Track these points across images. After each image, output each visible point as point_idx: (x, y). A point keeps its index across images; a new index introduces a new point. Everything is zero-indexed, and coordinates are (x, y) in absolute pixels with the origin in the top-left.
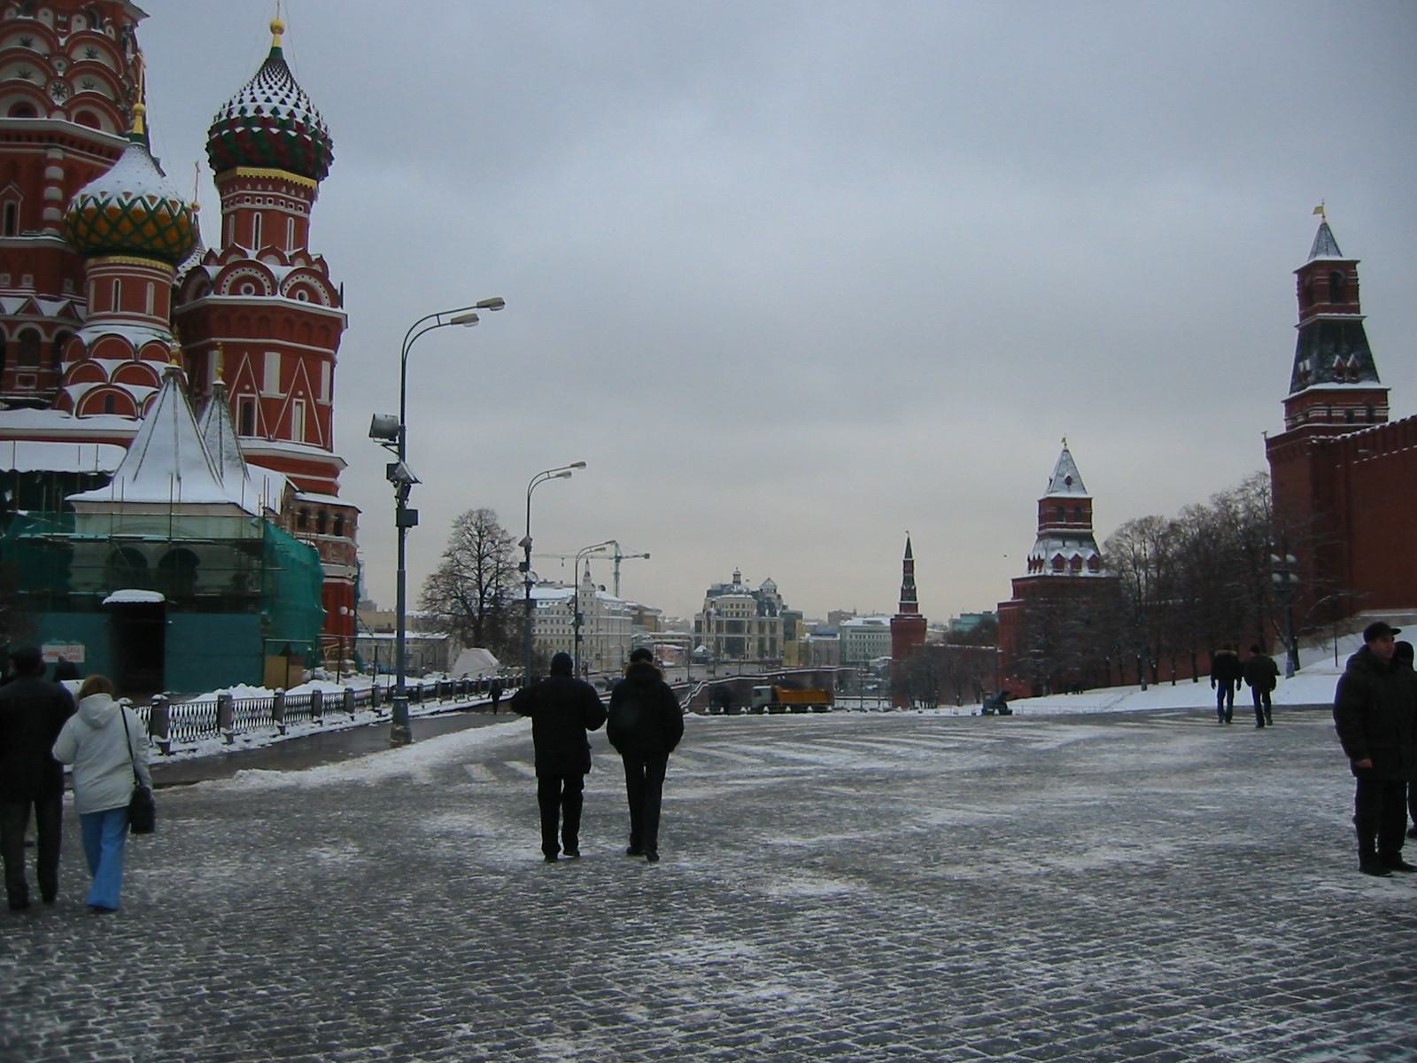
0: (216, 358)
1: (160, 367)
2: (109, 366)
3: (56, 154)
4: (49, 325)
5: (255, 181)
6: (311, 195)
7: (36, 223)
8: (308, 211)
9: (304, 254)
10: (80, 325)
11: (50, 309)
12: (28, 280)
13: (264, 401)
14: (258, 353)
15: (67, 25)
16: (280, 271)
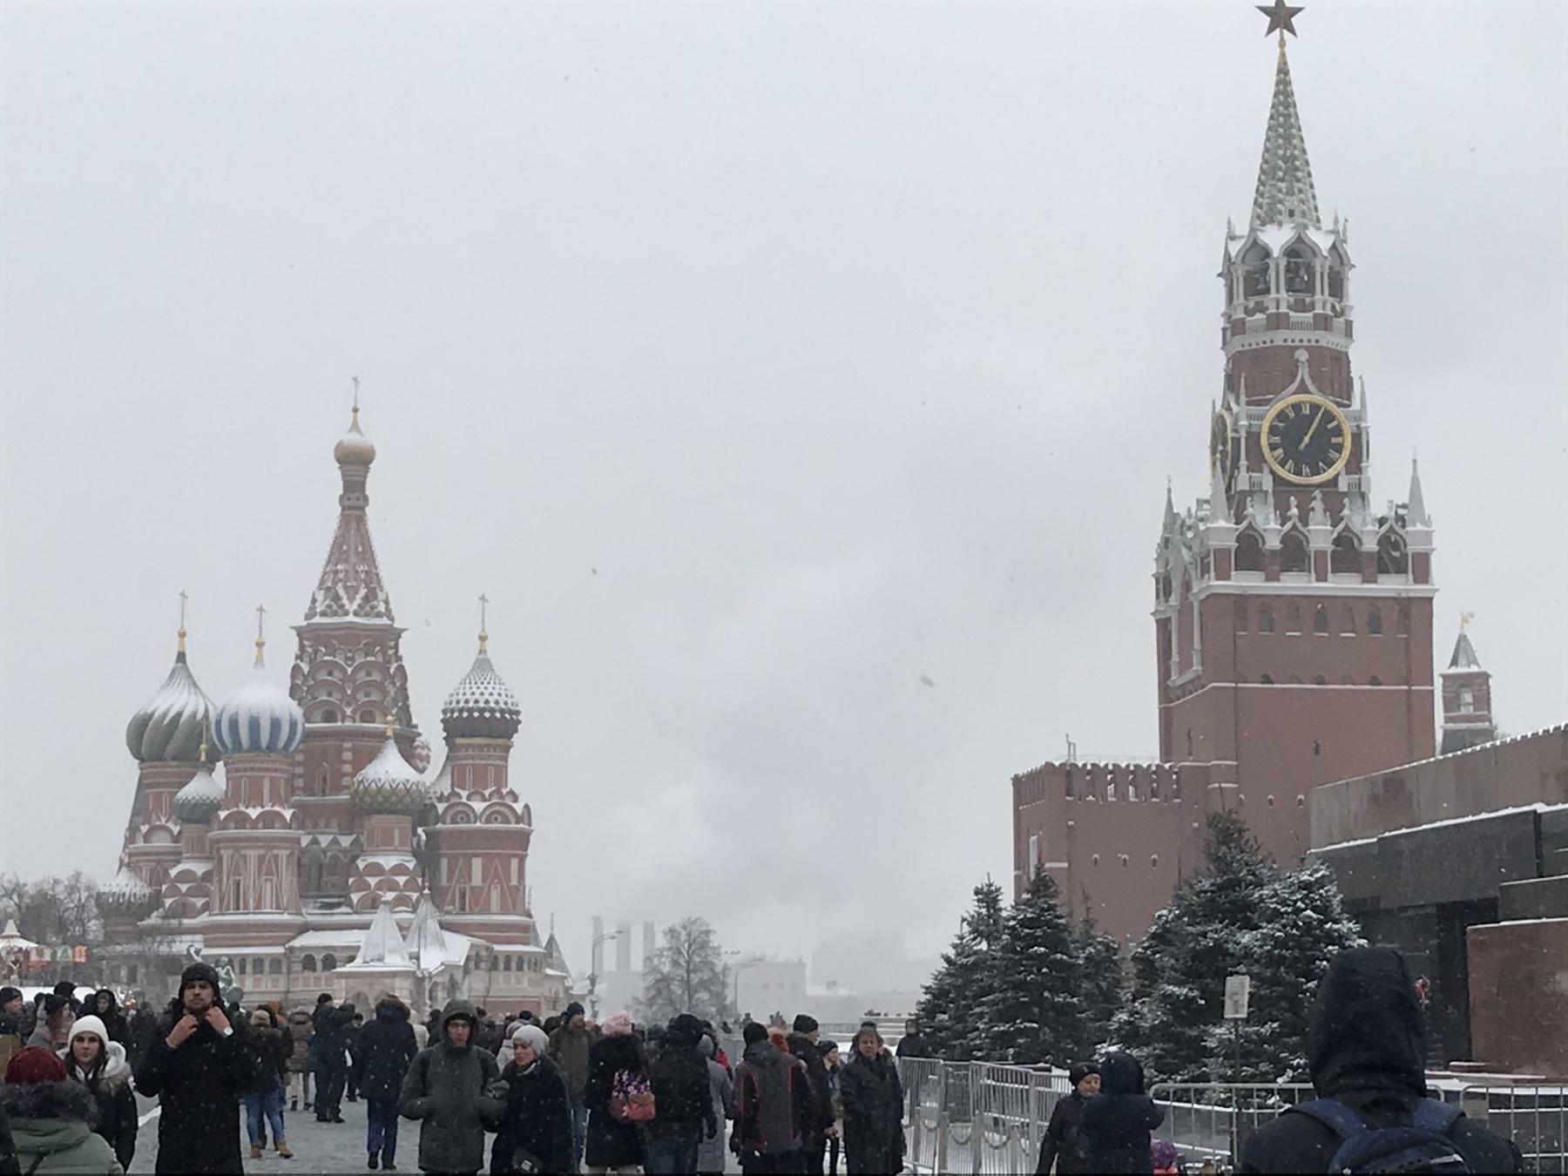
0: (444, 862)
1: (401, 880)
2: (372, 881)
3: (348, 745)
4: (344, 851)
5: (467, 747)
6: (507, 749)
7: (338, 789)
8: (506, 759)
9: (498, 792)
10: (363, 852)
11: (346, 841)
12: (334, 821)
13: (472, 888)
14: (468, 859)
15: (352, 659)
16: (478, 806)
